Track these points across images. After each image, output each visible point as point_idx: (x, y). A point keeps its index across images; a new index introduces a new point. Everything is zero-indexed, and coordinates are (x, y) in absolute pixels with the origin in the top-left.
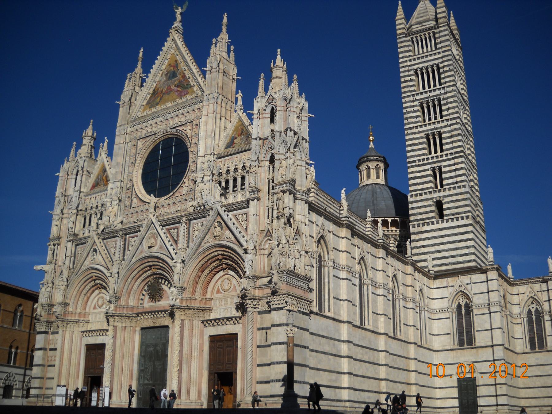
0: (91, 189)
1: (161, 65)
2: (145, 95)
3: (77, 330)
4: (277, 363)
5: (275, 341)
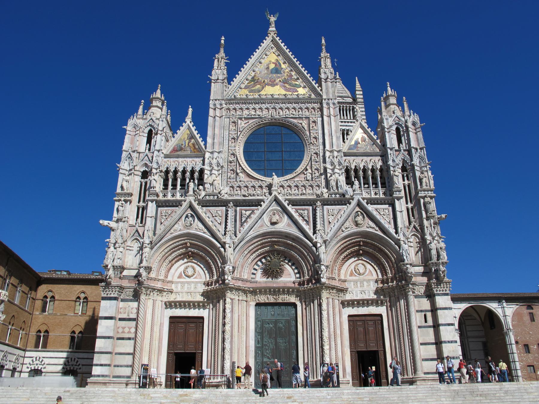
0: (170, 152)
1: (259, 58)
2: (243, 79)
3: (160, 299)
4: (449, 342)
5: (443, 323)
